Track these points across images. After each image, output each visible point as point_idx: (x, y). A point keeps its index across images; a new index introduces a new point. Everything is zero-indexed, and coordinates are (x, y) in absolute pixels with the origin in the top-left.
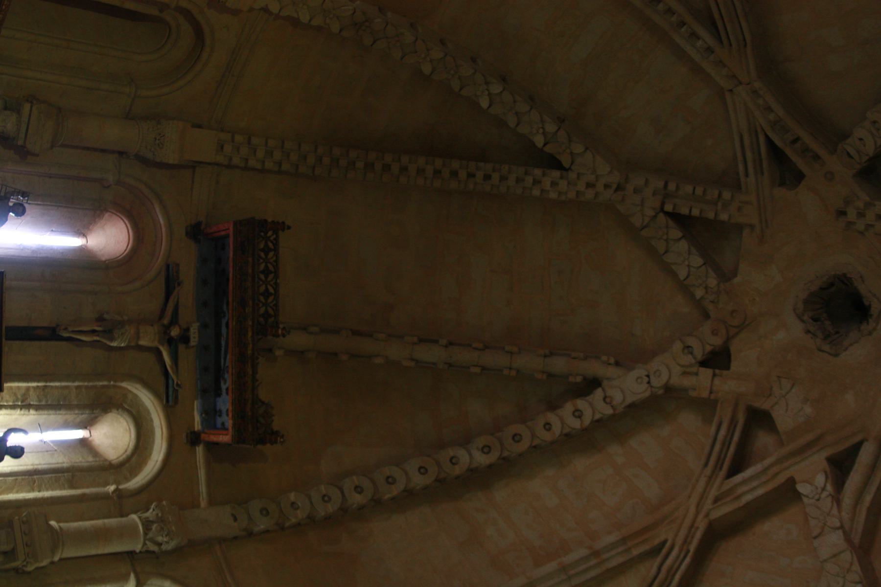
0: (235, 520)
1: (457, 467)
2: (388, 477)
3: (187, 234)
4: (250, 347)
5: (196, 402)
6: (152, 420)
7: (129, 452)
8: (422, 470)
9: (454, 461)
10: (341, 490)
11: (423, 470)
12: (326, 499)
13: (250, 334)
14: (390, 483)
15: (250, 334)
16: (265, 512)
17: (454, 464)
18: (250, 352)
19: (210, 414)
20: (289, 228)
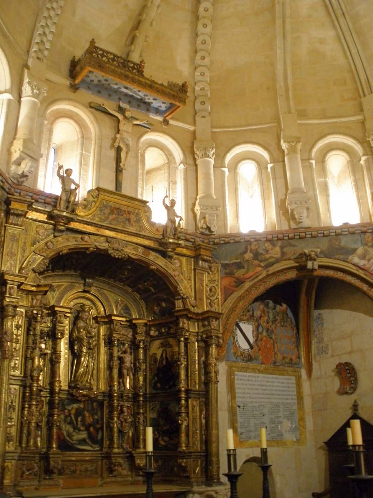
0: (204, 117)
1: (209, 10)
2: (202, 43)
3: (74, 92)
4: (147, 81)
5: (150, 116)
6: (151, 139)
7: (163, 154)
8: (205, 26)
9: (206, 10)
10: (200, 66)
11: (205, 26)
12: (203, 74)
13: (141, 79)
14: (205, 43)
15: (141, 79)
16: (203, 103)
17: (208, 10)
18: (149, 83)
19: (157, 111)
20: (93, 39)
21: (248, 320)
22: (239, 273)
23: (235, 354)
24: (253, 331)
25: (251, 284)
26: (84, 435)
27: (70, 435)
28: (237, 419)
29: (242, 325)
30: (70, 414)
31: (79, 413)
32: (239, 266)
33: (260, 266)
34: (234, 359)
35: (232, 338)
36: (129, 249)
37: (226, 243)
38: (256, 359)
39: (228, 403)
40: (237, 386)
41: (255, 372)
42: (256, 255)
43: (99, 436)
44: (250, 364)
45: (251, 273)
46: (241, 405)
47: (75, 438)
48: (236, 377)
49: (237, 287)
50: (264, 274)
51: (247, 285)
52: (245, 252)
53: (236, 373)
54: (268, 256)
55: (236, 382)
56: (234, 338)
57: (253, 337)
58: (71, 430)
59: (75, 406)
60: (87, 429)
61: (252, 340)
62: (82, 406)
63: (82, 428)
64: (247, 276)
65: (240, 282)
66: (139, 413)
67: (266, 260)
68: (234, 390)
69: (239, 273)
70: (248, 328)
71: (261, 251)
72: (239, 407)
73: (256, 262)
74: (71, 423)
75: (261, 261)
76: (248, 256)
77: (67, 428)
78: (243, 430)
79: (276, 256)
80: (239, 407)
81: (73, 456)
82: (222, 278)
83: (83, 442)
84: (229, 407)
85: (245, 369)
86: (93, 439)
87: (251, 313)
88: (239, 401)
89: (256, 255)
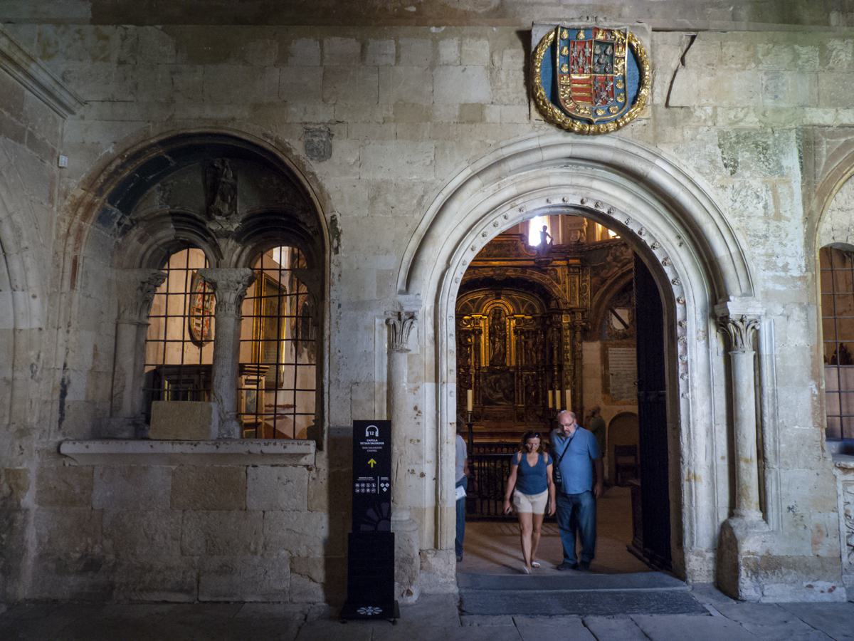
21: (623, 306)
22: (603, 274)
23: (609, 334)
24: (629, 314)
25: (611, 281)
26: (500, 395)
27: (490, 395)
28: (609, 384)
29: (617, 311)
30: (490, 382)
31: (497, 381)
32: (603, 267)
33: (616, 266)
34: (608, 338)
35: (607, 322)
36: (511, 272)
37: (596, 249)
38: (631, 336)
39: (602, 371)
40: (610, 359)
41: (630, 347)
42: (615, 259)
43: (512, 396)
44: (625, 341)
45: (611, 273)
46: (615, 373)
47: (494, 397)
48: (610, 352)
49: (602, 284)
50: (620, 273)
51: (609, 282)
52: (607, 256)
53: (609, 349)
54: (622, 258)
55: (610, 355)
56: (608, 321)
57: (629, 319)
58: (492, 392)
59: (494, 376)
60: (503, 390)
61: (627, 322)
62: (499, 376)
63: (500, 391)
64: (609, 275)
65: (603, 281)
66: (539, 380)
67: (620, 261)
68: (608, 361)
69: (603, 274)
70: (624, 314)
71: (618, 254)
72: (612, 374)
73: (615, 263)
74: (491, 388)
75: (618, 262)
76: (609, 258)
77: (488, 391)
78: (615, 392)
79: (628, 257)
80: (612, 374)
81: (496, 409)
82: (591, 278)
83: (500, 399)
84: (602, 375)
85: (619, 346)
86: (507, 397)
87: (627, 299)
88: (612, 370)
89: (615, 259)
